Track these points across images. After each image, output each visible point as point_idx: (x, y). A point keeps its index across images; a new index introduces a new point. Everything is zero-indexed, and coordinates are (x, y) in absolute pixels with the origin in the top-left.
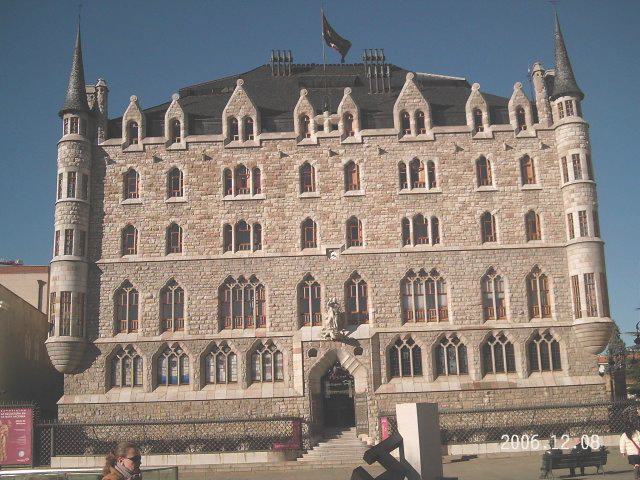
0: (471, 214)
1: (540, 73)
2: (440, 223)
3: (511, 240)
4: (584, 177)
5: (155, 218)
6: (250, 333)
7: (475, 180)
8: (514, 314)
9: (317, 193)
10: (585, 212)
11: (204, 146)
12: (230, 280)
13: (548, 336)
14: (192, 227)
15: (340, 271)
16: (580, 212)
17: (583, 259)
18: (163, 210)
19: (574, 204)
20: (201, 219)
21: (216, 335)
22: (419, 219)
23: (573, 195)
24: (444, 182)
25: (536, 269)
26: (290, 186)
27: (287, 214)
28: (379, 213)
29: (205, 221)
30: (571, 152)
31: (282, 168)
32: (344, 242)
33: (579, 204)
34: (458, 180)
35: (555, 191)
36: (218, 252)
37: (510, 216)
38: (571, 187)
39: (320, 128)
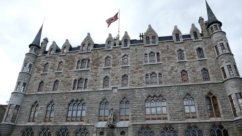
0: (176, 71)
2: (163, 75)
3: (195, 81)
5: (51, 79)
6: (76, 124)
9: (111, 67)
11: (72, 54)
12: (73, 101)
13: (221, 127)
14: (62, 81)
15: (117, 97)
17: (233, 86)
18: (54, 75)
19: (223, 63)
20: (66, 78)
21: (63, 124)
23: (222, 59)
24: (164, 60)
25: (210, 93)
26: (101, 65)
27: (98, 75)
28: (135, 73)
29: (67, 79)
30: (219, 43)
31: (98, 59)
32: (120, 85)
33: (226, 62)
34: (169, 58)
35: (214, 60)
36: (69, 90)
37: (194, 71)
38: (221, 56)
39: (115, 45)
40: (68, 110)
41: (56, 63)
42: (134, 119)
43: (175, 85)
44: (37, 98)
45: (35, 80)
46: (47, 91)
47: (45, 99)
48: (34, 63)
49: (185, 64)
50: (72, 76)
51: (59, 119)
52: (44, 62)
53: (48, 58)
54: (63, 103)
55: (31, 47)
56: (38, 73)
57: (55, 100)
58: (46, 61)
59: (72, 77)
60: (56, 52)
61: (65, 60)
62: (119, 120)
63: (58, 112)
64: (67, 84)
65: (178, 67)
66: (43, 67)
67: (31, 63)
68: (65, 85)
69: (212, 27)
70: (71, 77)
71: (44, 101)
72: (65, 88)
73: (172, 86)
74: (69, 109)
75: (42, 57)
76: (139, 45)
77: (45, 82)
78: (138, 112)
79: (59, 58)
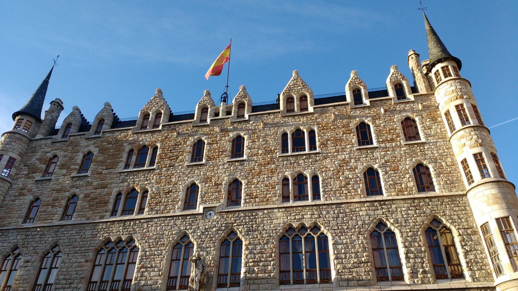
1: (413, 56)
4: (472, 122)
5: (58, 191)
7: (355, 140)
8: (414, 274)
10: (480, 154)
12: (108, 241)
14: (86, 196)
15: (214, 229)
16: (475, 155)
20: (96, 189)
22: (300, 179)
23: (463, 141)
24: (324, 144)
27: (174, 180)
29: (98, 191)
33: (472, 147)
34: (337, 141)
36: (102, 217)
40: (94, 266)
41: (75, 154)
42: (252, 281)
43: (349, 201)
44: (19, 237)
45: (21, 194)
46: (49, 221)
47: (37, 239)
48: (21, 155)
49: (372, 153)
50: (111, 183)
51: (69, 288)
52: (48, 152)
53: (58, 144)
54: (83, 249)
55: (17, 118)
56: (29, 178)
57: (63, 240)
58: (52, 150)
59: (113, 185)
60: (78, 132)
61: (97, 149)
62: (214, 284)
63: (67, 271)
64: (97, 203)
65: (357, 160)
66: (44, 164)
67: (14, 156)
68: (93, 206)
69: (438, 71)
70: (109, 186)
71: (34, 246)
72: (91, 212)
73: (342, 203)
74: (97, 263)
75: (43, 142)
76: (269, 114)
77: (43, 199)
78: (261, 264)
79: (84, 143)
